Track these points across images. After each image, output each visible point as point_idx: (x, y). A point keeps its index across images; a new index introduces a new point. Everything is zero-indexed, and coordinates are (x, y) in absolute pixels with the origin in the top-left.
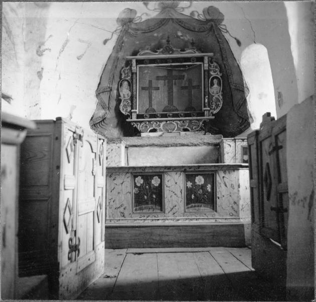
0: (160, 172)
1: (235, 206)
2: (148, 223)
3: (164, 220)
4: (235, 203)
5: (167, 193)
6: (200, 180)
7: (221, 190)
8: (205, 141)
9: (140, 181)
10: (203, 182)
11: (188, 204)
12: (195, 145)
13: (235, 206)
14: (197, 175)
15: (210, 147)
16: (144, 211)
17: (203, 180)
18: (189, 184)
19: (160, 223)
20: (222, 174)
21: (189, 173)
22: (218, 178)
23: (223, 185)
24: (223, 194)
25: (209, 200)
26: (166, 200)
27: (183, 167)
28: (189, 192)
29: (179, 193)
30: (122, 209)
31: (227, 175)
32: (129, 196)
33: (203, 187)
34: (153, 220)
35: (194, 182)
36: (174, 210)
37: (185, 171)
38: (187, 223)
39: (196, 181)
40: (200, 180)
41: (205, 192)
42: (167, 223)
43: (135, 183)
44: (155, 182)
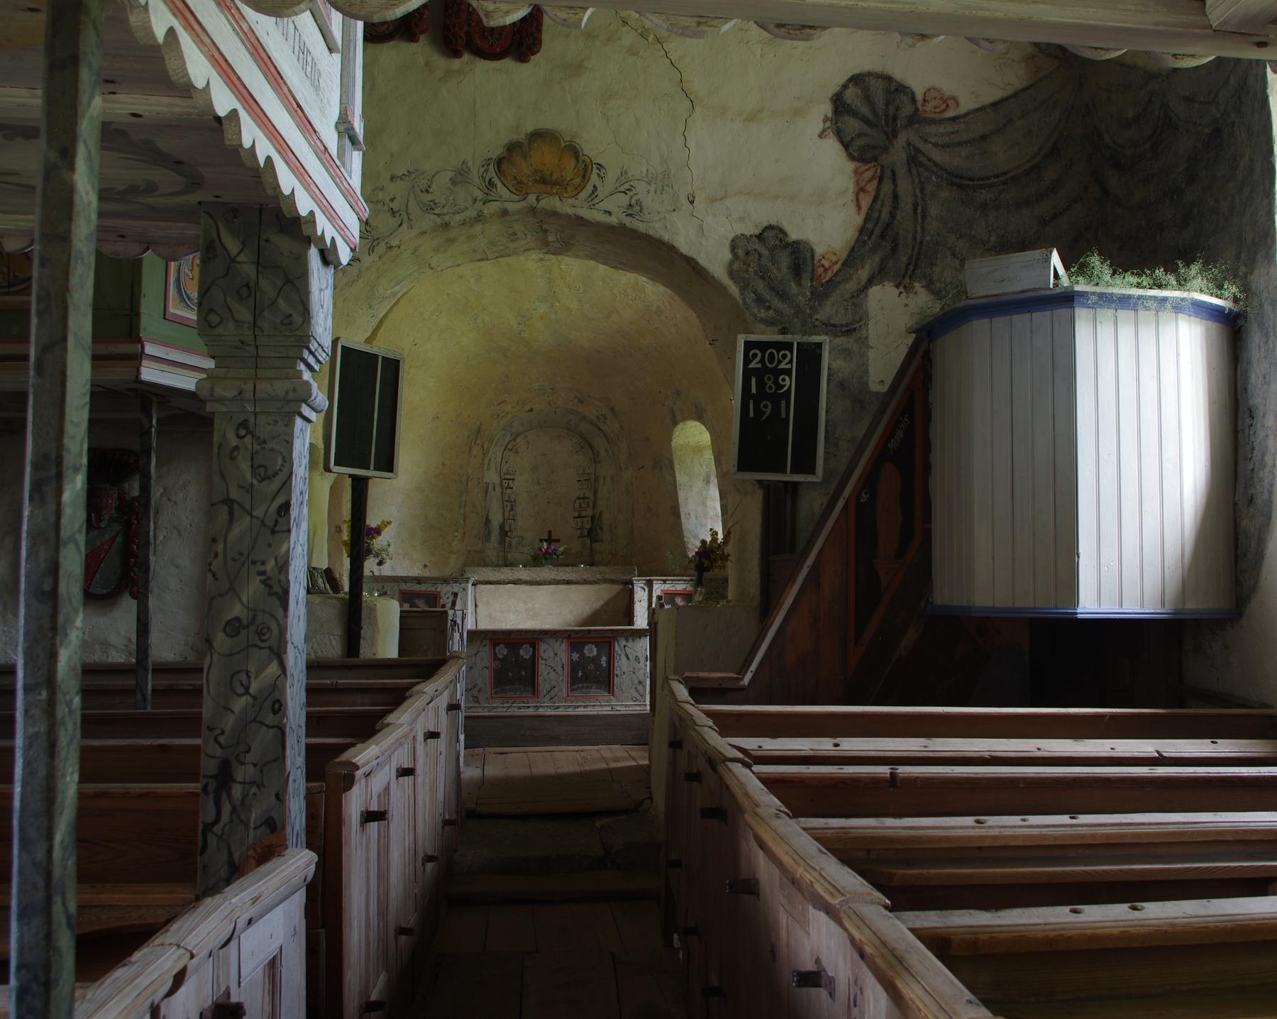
0: (533, 638)
1: (640, 687)
2: (515, 711)
3: (537, 707)
4: (640, 683)
5: (542, 669)
6: (591, 651)
7: (622, 664)
8: (608, 576)
9: (502, 651)
10: (595, 653)
11: (573, 684)
12: (590, 583)
13: (640, 687)
14: (587, 643)
15: (616, 588)
16: (508, 694)
17: (595, 650)
18: (575, 656)
19: (531, 712)
20: (623, 642)
21: (573, 638)
22: (617, 648)
23: (624, 658)
24: (624, 669)
25: (605, 680)
26: (541, 679)
27: (566, 631)
28: (574, 667)
29: (559, 670)
30: (475, 692)
31: (630, 644)
32: (487, 673)
33: (595, 660)
34: (520, 708)
35: (581, 651)
36: (552, 693)
37: (569, 637)
38: (571, 712)
39: (586, 651)
40: (591, 651)
41: (599, 666)
42: (542, 711)
43: (495, 654)
44: (525, 652)
